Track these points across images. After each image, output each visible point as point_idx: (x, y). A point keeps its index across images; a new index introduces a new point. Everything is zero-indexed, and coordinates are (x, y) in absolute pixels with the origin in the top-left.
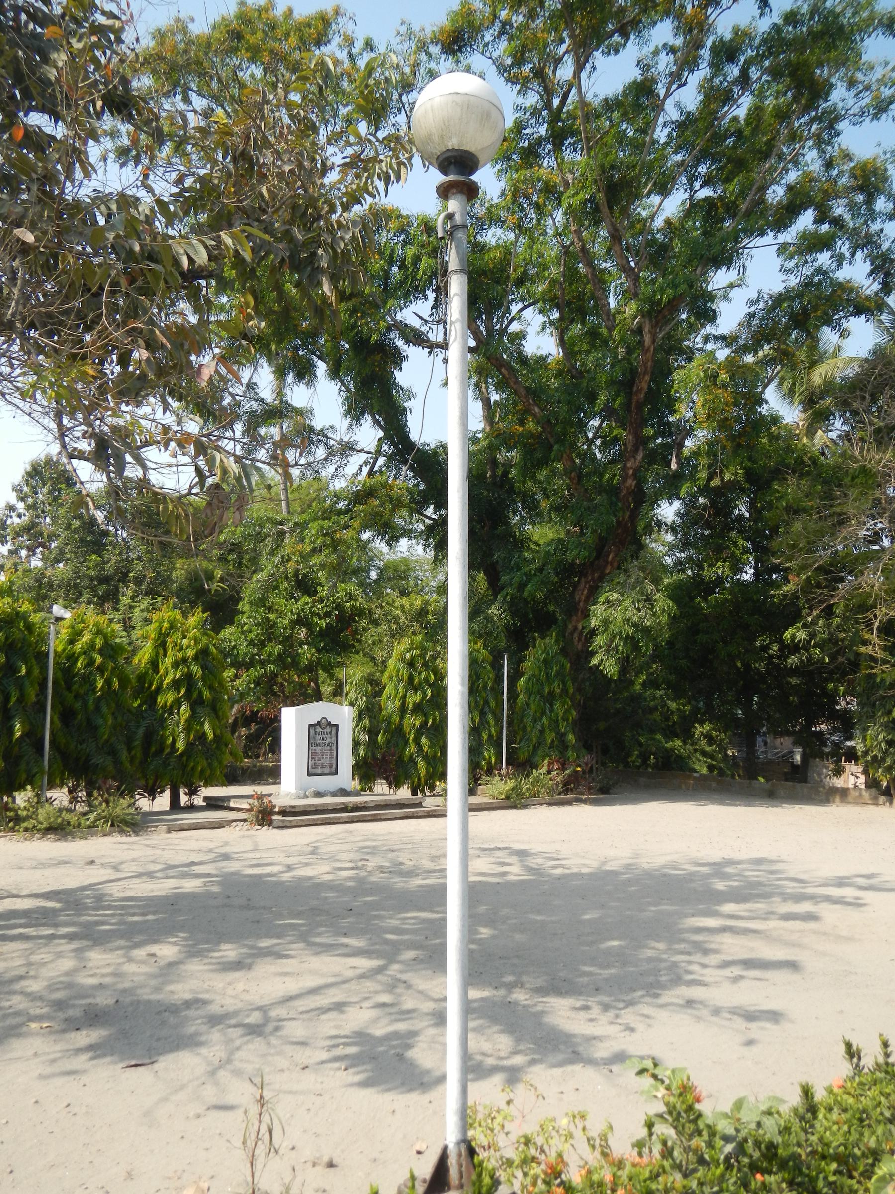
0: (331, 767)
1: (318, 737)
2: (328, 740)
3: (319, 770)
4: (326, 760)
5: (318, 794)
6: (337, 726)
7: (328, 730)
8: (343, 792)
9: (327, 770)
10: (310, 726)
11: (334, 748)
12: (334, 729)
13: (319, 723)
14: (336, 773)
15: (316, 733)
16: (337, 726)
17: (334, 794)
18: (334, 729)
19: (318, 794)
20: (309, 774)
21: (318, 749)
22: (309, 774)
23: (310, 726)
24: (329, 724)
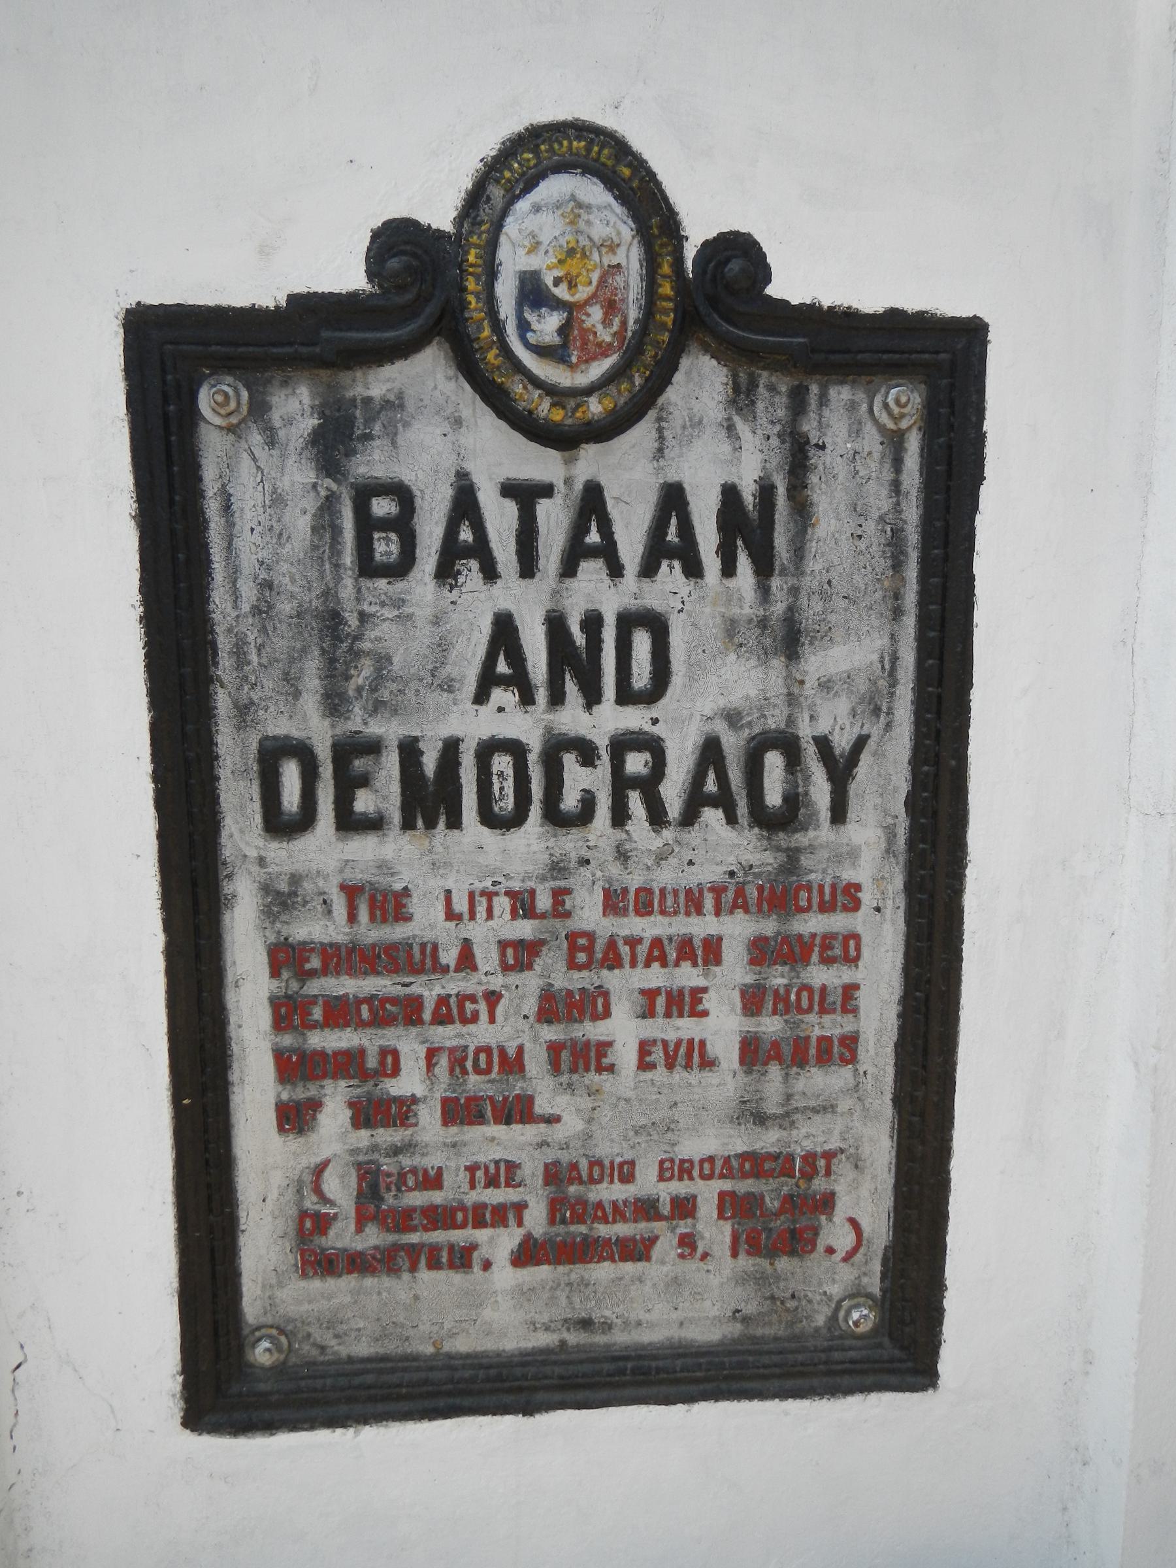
1: (436, 622)
2: (712, 690)
3: (500, 1306)
4: (665, 1108)
6: (939, 361)
9: (687, 1295)
10: (176, 361)
11: (865, 845)
12: (860, 439)
13: (422, 286)
14: (900, 1344)
15: (375, 529)
16: (939, 361)
18: (860, 439)
22: (231, 1379)
23: (176, 361)
24: (718, 300)
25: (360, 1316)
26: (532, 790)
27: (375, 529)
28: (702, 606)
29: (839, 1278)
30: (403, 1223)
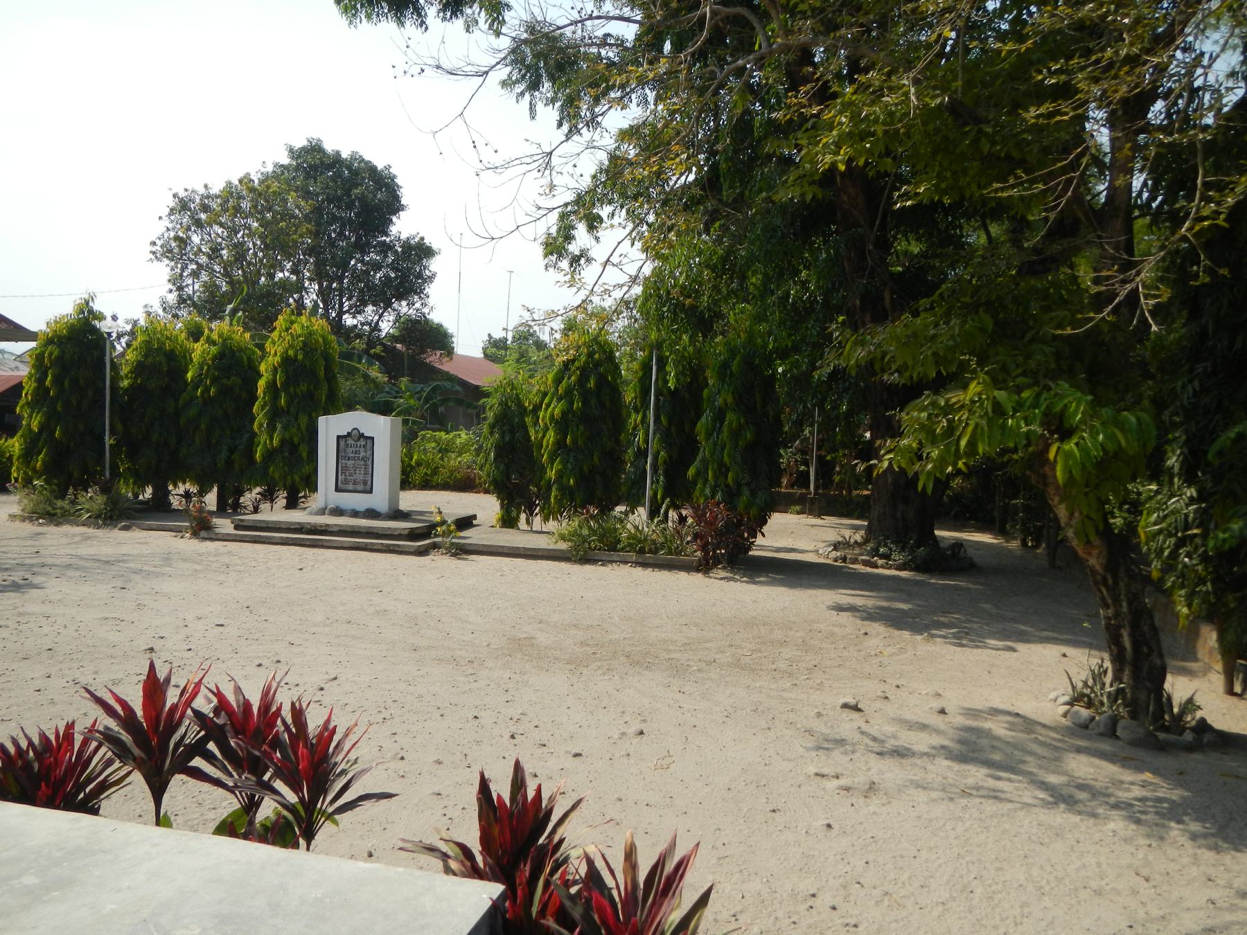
0: (365, 483)
2: (362, 454)
3: (351, 487)
4: (359, 476)
5: (338, 512)
7: (362, 442)
8: (372, 514)
9: (360, 487)
10: (339, 437)
13: (349, 434)
14: (371, 492)
15: (347, 446)
17: (355, 514)
18: (369, 442)
19: (338, 512)
20: (337, 490)
21: (350, 463)
22: (337, 490)
23: (339, 437)
24: (362, 435)
25: (344, 487)
26: (354, 459)
27: (347, 446)
28: (362, 450)
29: (368, 487)
30: (346, 482)
